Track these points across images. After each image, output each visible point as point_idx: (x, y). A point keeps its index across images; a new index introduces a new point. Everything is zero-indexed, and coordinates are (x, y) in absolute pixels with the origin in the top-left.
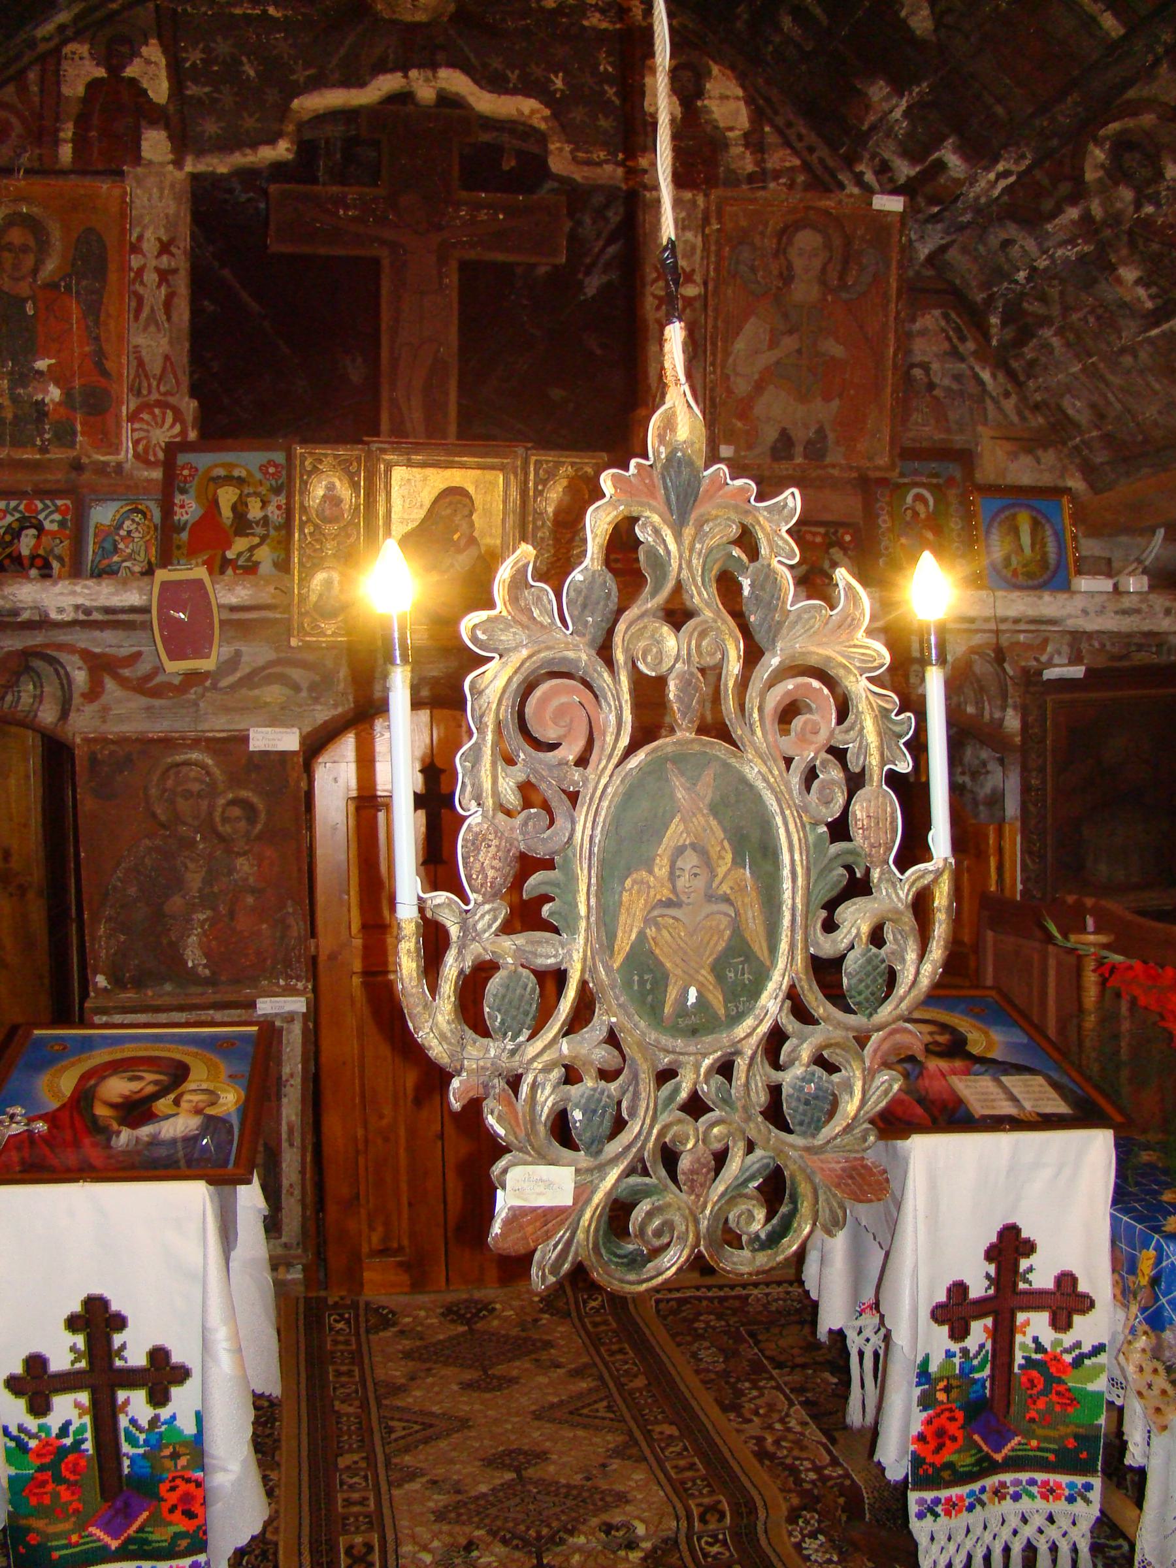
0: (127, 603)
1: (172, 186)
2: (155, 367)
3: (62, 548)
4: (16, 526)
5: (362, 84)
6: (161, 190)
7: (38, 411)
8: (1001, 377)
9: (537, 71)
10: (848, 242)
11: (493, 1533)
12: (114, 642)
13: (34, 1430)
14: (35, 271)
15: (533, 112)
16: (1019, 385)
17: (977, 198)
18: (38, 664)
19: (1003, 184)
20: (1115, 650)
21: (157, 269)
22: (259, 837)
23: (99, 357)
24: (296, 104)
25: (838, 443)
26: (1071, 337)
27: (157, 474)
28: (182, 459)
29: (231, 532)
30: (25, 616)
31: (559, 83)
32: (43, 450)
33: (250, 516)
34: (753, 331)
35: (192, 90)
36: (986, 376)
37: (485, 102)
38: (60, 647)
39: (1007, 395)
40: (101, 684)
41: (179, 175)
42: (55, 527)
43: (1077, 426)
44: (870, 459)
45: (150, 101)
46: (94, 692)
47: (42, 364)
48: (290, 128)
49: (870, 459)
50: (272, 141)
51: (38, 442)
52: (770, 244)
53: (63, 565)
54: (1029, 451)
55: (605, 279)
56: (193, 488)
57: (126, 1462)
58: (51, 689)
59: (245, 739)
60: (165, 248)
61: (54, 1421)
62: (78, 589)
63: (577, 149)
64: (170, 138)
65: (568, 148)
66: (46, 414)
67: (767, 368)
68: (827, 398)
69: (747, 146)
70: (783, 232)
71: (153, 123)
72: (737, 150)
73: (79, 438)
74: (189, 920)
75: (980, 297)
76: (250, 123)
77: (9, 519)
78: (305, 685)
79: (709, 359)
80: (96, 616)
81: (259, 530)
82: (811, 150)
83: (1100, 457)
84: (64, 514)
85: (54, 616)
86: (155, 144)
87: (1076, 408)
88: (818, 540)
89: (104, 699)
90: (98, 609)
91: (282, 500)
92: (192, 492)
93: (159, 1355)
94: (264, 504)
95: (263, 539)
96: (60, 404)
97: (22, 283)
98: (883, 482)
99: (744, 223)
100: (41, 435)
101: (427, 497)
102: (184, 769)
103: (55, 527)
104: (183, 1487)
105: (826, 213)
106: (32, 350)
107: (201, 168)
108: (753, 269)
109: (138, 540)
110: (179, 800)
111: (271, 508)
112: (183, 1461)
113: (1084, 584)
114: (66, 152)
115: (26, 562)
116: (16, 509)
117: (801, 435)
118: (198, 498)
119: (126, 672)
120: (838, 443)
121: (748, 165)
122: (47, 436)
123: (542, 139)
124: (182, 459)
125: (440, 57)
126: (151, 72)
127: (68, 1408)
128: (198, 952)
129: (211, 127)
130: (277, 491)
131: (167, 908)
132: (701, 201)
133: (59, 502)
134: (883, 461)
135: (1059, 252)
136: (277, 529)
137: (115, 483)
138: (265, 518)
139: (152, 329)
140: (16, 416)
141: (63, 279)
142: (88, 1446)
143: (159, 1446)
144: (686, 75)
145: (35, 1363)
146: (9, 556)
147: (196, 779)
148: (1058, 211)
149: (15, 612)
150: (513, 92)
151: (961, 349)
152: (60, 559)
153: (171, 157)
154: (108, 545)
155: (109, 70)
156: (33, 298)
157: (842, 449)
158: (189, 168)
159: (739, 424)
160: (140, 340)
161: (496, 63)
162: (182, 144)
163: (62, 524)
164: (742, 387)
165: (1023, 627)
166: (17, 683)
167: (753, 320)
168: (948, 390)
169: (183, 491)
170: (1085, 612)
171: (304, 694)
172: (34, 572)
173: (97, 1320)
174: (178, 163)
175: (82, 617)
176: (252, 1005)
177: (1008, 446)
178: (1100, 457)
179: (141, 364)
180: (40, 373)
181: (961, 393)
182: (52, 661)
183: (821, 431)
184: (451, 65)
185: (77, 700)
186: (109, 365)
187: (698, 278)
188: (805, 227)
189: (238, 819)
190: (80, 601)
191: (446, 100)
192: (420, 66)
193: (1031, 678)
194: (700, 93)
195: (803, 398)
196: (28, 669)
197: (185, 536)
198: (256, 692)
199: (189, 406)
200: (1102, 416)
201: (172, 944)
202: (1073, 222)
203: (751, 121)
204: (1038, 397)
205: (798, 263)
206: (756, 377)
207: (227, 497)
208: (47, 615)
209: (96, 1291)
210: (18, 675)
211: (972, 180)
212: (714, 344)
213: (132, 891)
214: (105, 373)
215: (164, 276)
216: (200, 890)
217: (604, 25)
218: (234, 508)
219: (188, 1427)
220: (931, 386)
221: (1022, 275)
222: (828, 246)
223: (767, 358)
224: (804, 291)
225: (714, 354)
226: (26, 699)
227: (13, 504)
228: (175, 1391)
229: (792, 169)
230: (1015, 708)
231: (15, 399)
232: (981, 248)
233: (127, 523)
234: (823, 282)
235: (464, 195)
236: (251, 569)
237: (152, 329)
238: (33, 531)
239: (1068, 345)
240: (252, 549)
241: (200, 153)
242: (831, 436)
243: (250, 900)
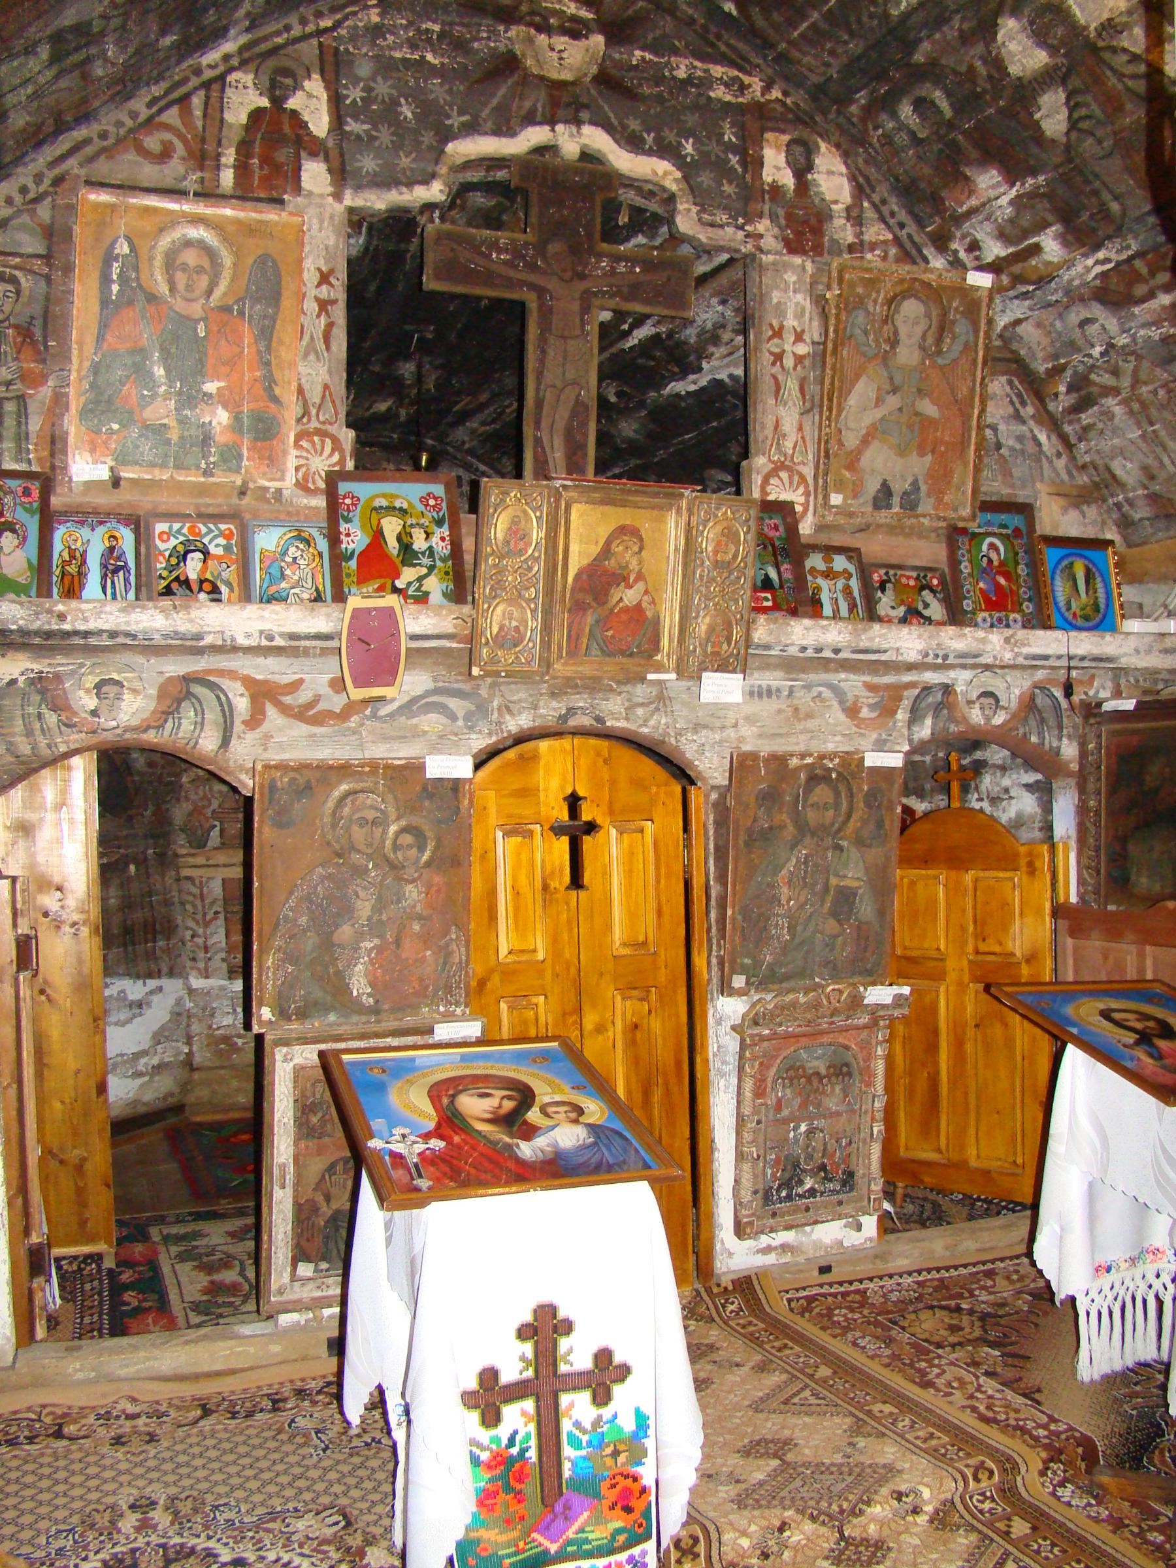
0: (313, 630)
1: (332, 217)
2: (315, 396)
3: (230, 573)
4: (181, 549)
5: (512, 133)
6: (321, 222)
8: (1054, 438)
9: (670, 136)
10: (944, 315)
11: (801, 1512)
12: (276, 668)
13: (486, 1441)
14: (209, 293)
15: (666, 173)
16: (1069, 446)
17: (1071, 280)
18: (197, 689)
19: (1099, 269)
20: (1147, 685)
21: (317, 299)
22: (428, 864)
23: (269, 383)
24: (450, 147)
25: (929, 495)
26: (1136, 406)
27: (320, 502)
28: (343, 487)
29: (398, 561)
30: (208, 640)
31: (689, 148)
32: (207, 473)
33: (415, 547)
34: (862, 391)
35: (352, 126)
36: (1043, 437)
37: (623, 161)
38: (222, 673)
39: (1059, 455)
40: (263, 713)
41: (339, 208)
42: (220, 551)
43: (1122, 485)
44: (955, 510)
45: (310, 134)
46: (255, 719)
47: (211, 387)
48: (443, 170)
49: (955, 510)
50: (426, 182)
52: (879, 310)
53: (232, 590)
54: (1077, 506)
55: (653, 331)
56: (356, 515)
57: (567, 1467)
58: (212, 715)
59: (422, 768)
60: (324, 279)
61: (503, 1431)
62: (266, 614)
63: (703, 210)
64: (330, 171)
65: (695, 209)
67: (873, 425)
68: (922, 454)
69: (848, 219)
70: (890, 302)
71: (313, 155)
72: (839, 222)
73: (245, 463)
74: (356, 949)
75: (1041, 367)
76: (405, 162)
77: (173, 542)
78: (461, 714)
79: (826, 414)
80: (279, 642)
81: (426, 561)
82: (902, 226)
83: (1141, 512)
84: (229, 537)
85: (242, 641)
86: (315, 174)
87: (1126, 470)
88: (912, 583)
89: (266, 726)
90: (282, 635)
91: (445, 531)
92: (356, 520)
93: (603, 1357)
94: (428, 535)
95: (431, 569)
98: (964, 531)
99: (860, 290)
101: (604, 532)
102: (361, 796)
103: (220, 551)
104: (623, 1483)
105: (928, 285)
106: (200, 371)
107: (359, 202)
108: (866, 333)
109: (307, 569)
110: (355, 828)
111: (435, 540)
112: (622, 1459)
113: (1133, 625)
114: (227, 178)
115: (195, 588)
116: (179, 531)
117: (898, 487)
118: (363, 527)
119: (287, 700)
120: (929, 495)
121: (848, 236)
123: (671, 199)
124: (343, 487)
125: (584, 115)
126: (312, 105)
127: (518, 1418)
128: (363, 981)
129: (368, 164)
130: (439, 523)
131: (336, 938)
132: (809, 266)
133: (223, 527)
134: (966, 512)
135: (1142, 332)
136: (443, 560)
137: (275, 508)
138: (430, 548)
139: (312, 357)
140: (181, 438)
142: (532, 1454)
143: (602, 1444)
144: (798, 150)
145: (489, 1376)
146: (177, 579)
147: (372, 807)
148: (1151, 295)
149: (199, 637)
150: (649, 153)
151: (1022, 412)
152: (229, 584)
153: (330, 189)
154: (275, 571)
155: (274, 100)
158: (350, 199)
160: (302, 368)
161: (634, 125)
162: (341, 176)
163: (228, 548)
164: (851, 441)
165: (1086, 664)
166: (177, 709)
167: (864, 379)
168: (1012, 449)
169: (348, 520)
170: (1137, 651)
171: (460, 723)
172: (203, 596)
173: (545, 1328)
174: (338, 196)
175: (265, 643)
176: (431, 1031)
177: (1061, 501)
178: (1141, 512)
179: (300, 391)
180: (210, 396)
181: (1023, 452)
182: (213, 686)
183: (915, 483)
184: (593, 123)
185: (238, 727)
186: (277, 391)
187: (806, 337)
189: (410, 846)
190: (267, 626)
191: (586, 156)
192: (566, 122)
193: (1091, 710)
194: (810, 167)
195: (902, 452)
196: (189, 694)
197: (353, 564)
198: (415, 721)
199: (348, 436)
200: (1152, 478)
201: (338, 973)
202: (1164, 308)
203: (853, 196)
204: (1087, 459)
205: (903, 331)
207: (391, 527)
208: (233, 639)
209: (545, 1299)
210: (179, 702)
211: (1069, 264)
212: (830, 400)
213: (303, 920)
214: (276, 400)
215: (324, 305)
216: (369, 919)
217: (728, 98)
218: (399, 539)
219: (628, 1424)
220: (999, 446)
221: (1097, 351)
222: (928, 315)
224: (907, 354)
225: (830, 409)
226: (187, 726)
227: (176, 526)
228: (617, 1390)
229: (885, 242)
230: (1069, 737)
231: (183, 421)
232: (1058, 324)
233: (292, 550)
234: (922, 348)
235: (605, 246)
236: (422, 599)
237: (312, 357)
238: (199, 555)
239: (1131, 412)
240: (420, 579)
241: (359, 188)
242: (924, 488)
243: (416, 927)
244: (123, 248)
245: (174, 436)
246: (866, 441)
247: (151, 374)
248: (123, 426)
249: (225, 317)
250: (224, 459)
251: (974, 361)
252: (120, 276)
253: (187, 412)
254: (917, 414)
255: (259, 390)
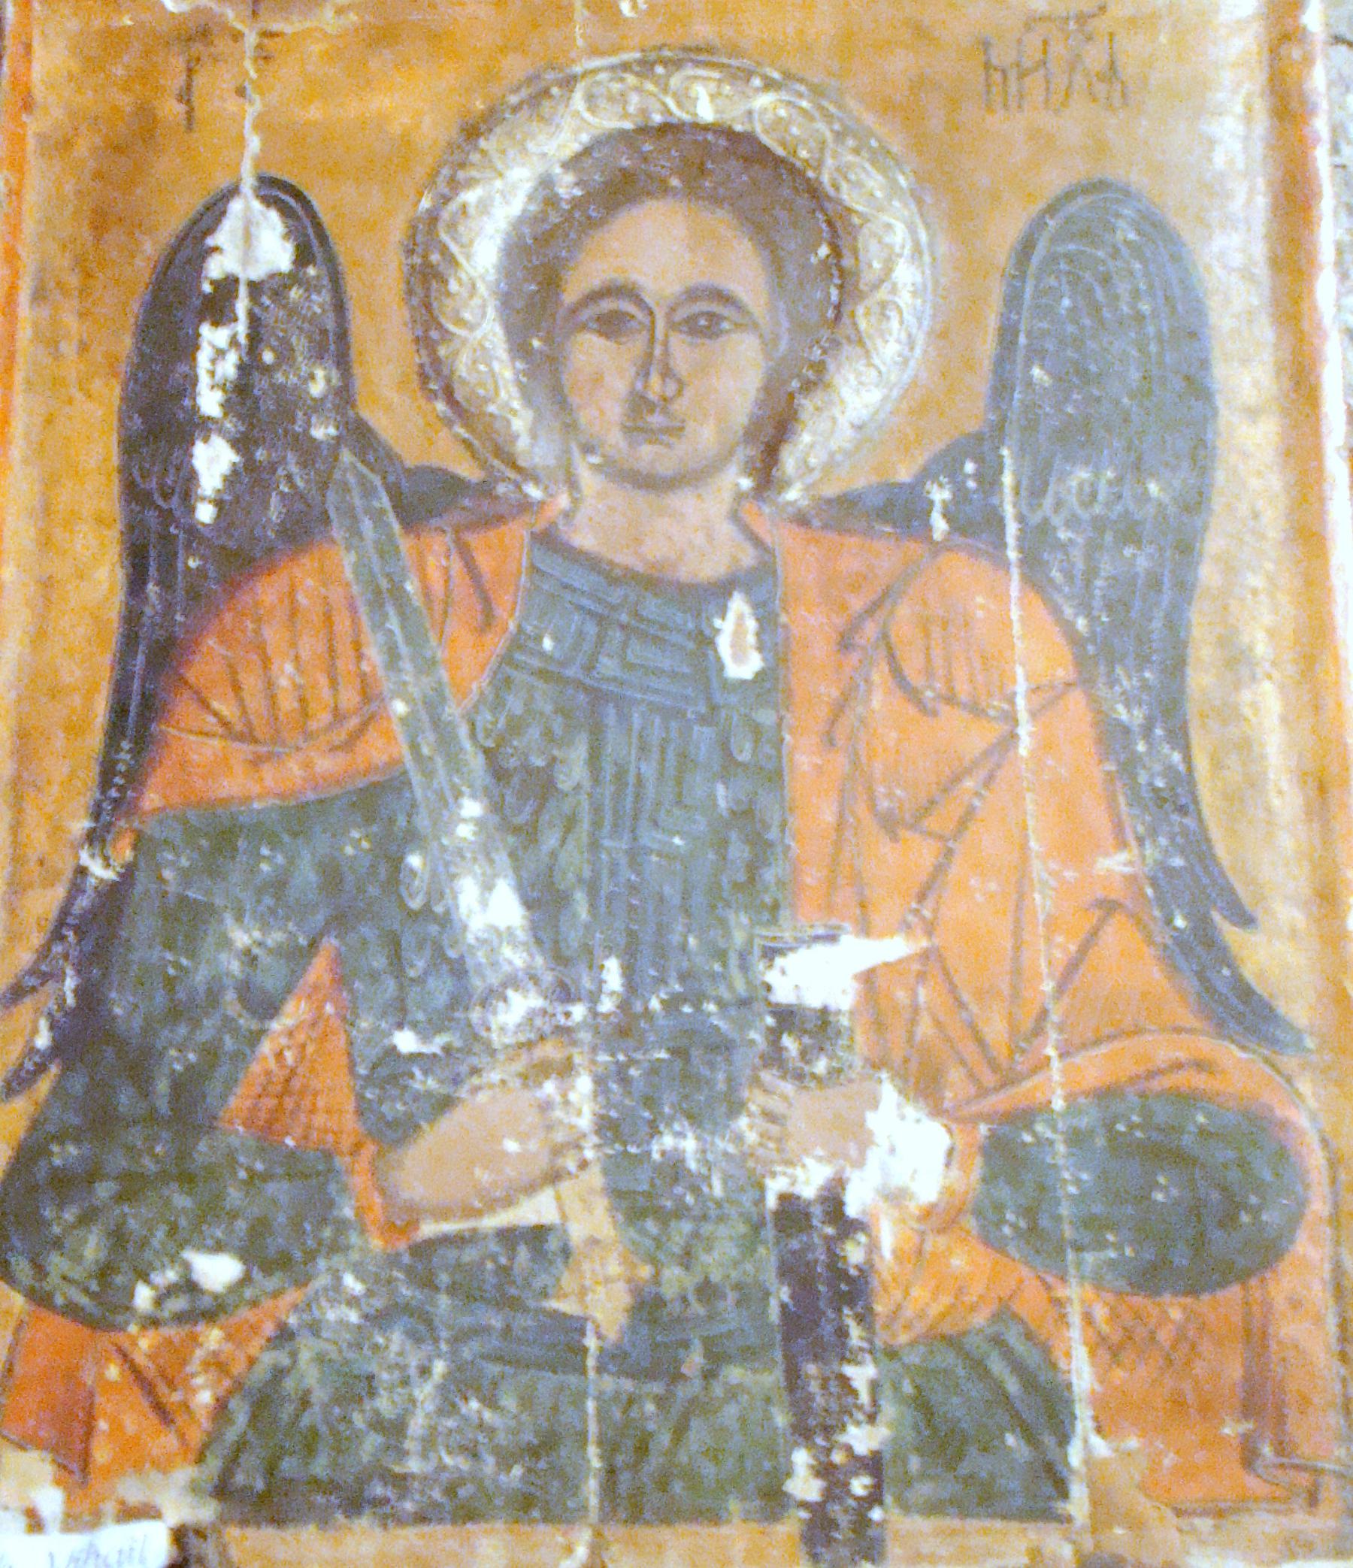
7: (793, 1270)
14: (771, 434)
51: (804, 1485)
66: (852, 1289)
73: (1087, 1446)
96: (941, 1218)
97: (683, 501)
100: (815, 1426)
106: (751, 874)
122: (861, 1439)
140: (647, 1307)
141: (946, 465)
156: (758, 580)
180: (818, 1026)
231: (647, 1200)
244: (254, 245)
245: (599, 1298)
247: (437, 920)
248: (255, 1253)
249: (882, 555)
250: (941, 1439)
252: (240, 393)
253: (681, 1142)
255: (1130, 963)
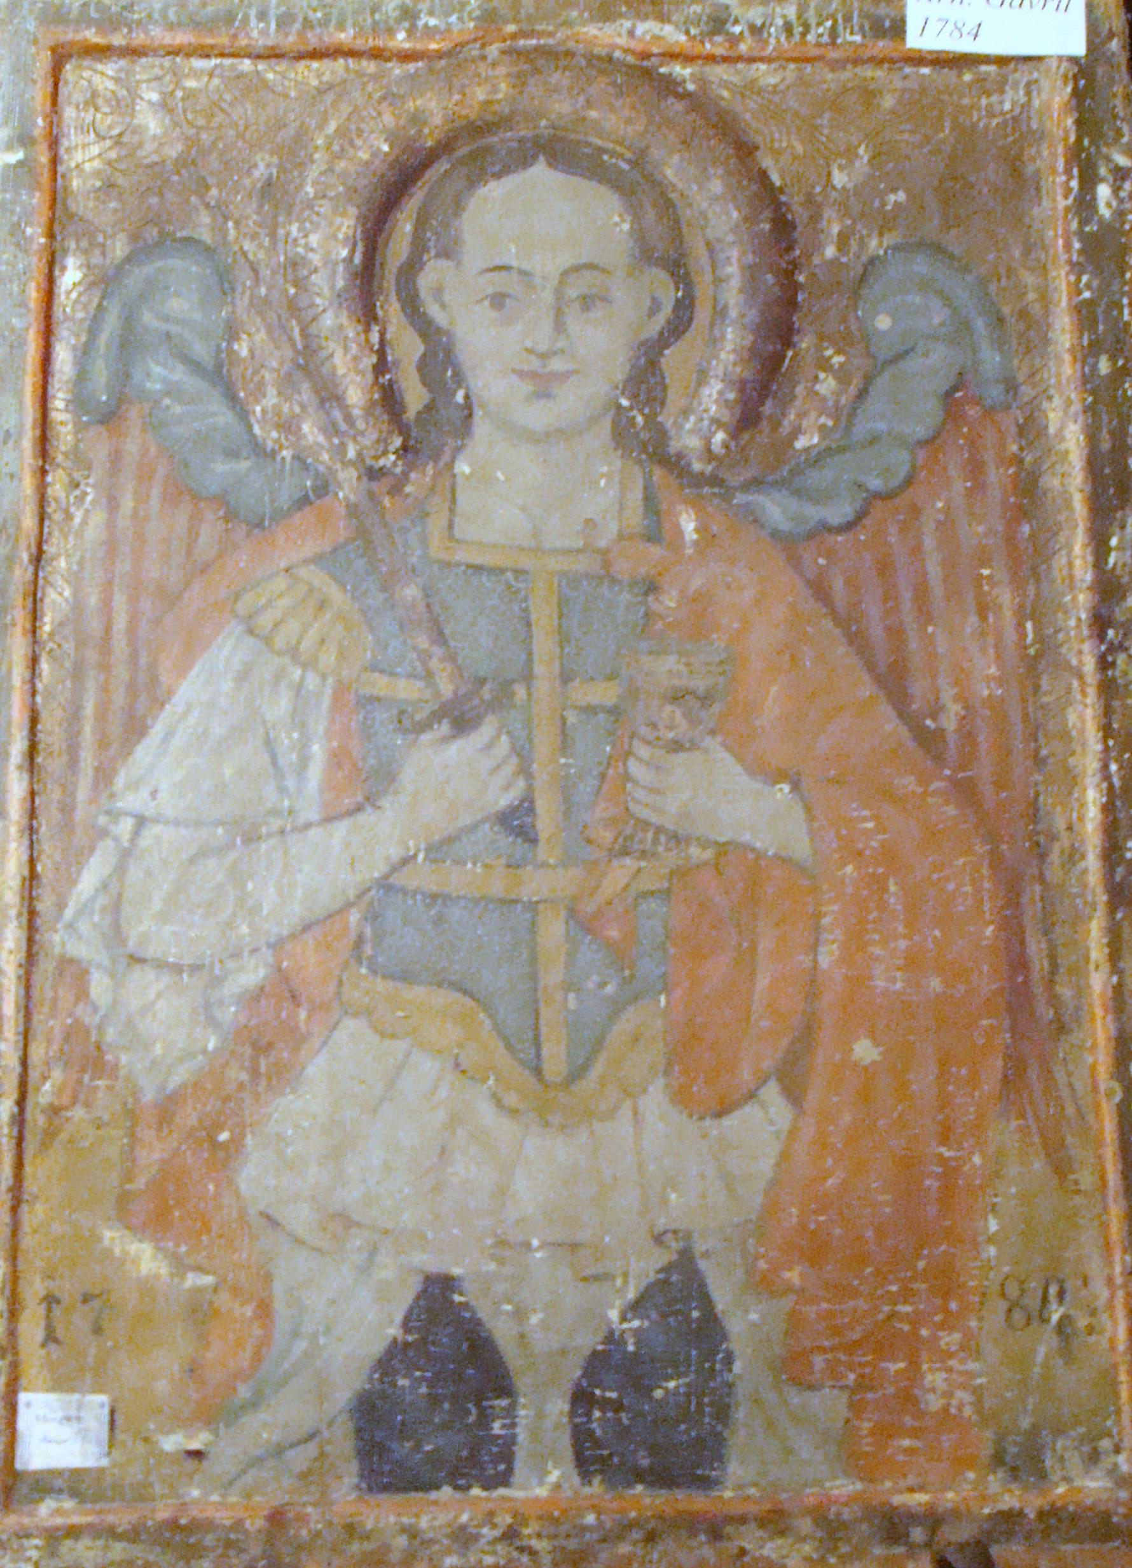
25: (793, 1369)
44: (1024, 1461)
49: (1024, 1461)
52: (326, 241)
70: (388, 195)
108: (222, 376)
117: (547, 1322)
120: (793, 1369)
157: (828, 1404)
159: (145, 1259)
167: (227, 650)
183: (680, 1299)
188: (521, 158)
195: (551, 1085)
205: (491, 352)
206: (253, 974)
222: (668, 253)
223: (322, 866)
234: (647, 446)
246: (267, 1046)
251: (1028, 493)
254: (631, 838)
